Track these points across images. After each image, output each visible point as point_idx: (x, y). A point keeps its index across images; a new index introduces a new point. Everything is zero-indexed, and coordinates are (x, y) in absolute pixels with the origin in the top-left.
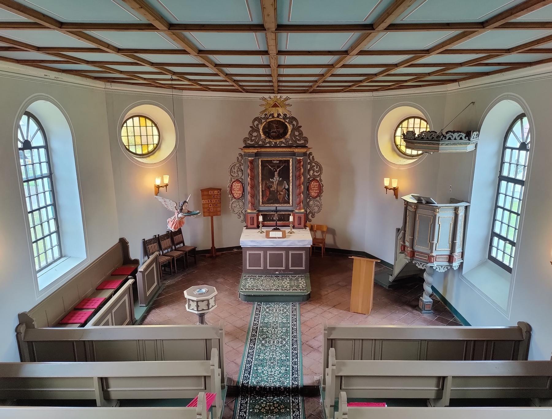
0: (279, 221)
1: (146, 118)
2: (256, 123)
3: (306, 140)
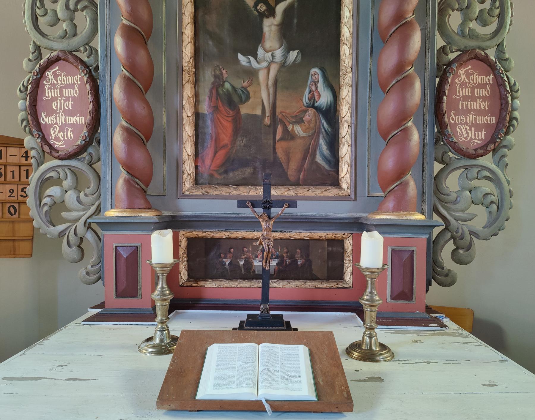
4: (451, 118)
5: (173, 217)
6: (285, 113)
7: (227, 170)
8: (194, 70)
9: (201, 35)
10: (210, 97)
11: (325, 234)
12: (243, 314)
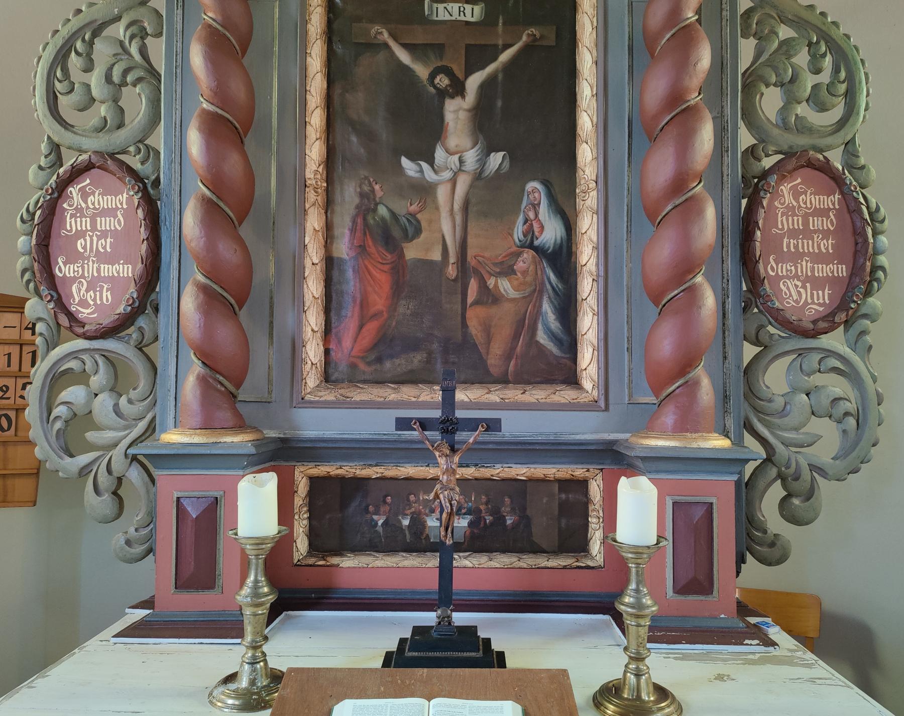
4: (770, 268)
5: (283, 440)
6: (483, 257)
7: (384, 356)
8: (325, 185)
9: (338, 126)
10: (353, 230)
11: (554, 470)
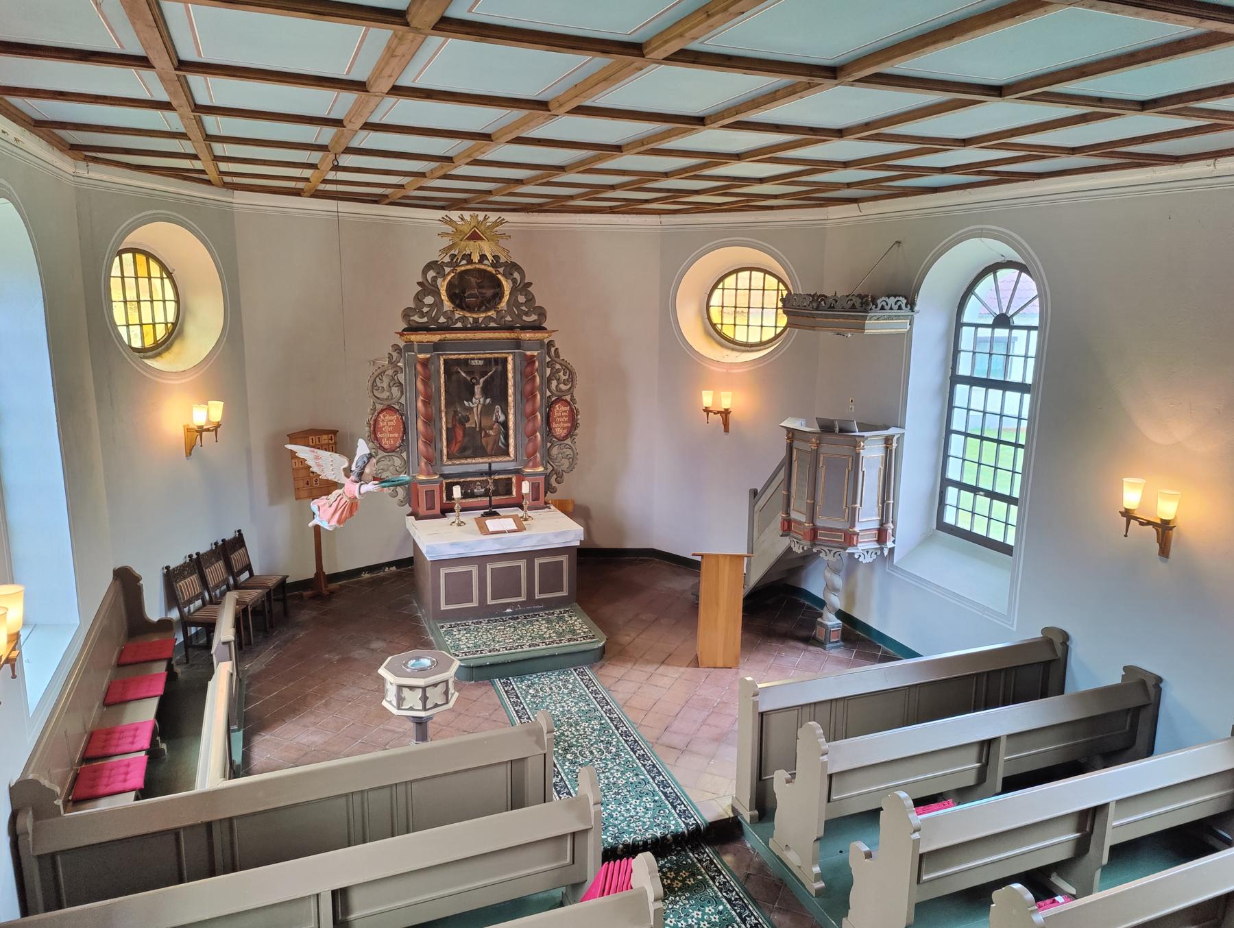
0: (497, 495)
1: (149, 255)
2: (431, 274)
3: (542, 313)
4: (554, 425)
12: (482, 512)
